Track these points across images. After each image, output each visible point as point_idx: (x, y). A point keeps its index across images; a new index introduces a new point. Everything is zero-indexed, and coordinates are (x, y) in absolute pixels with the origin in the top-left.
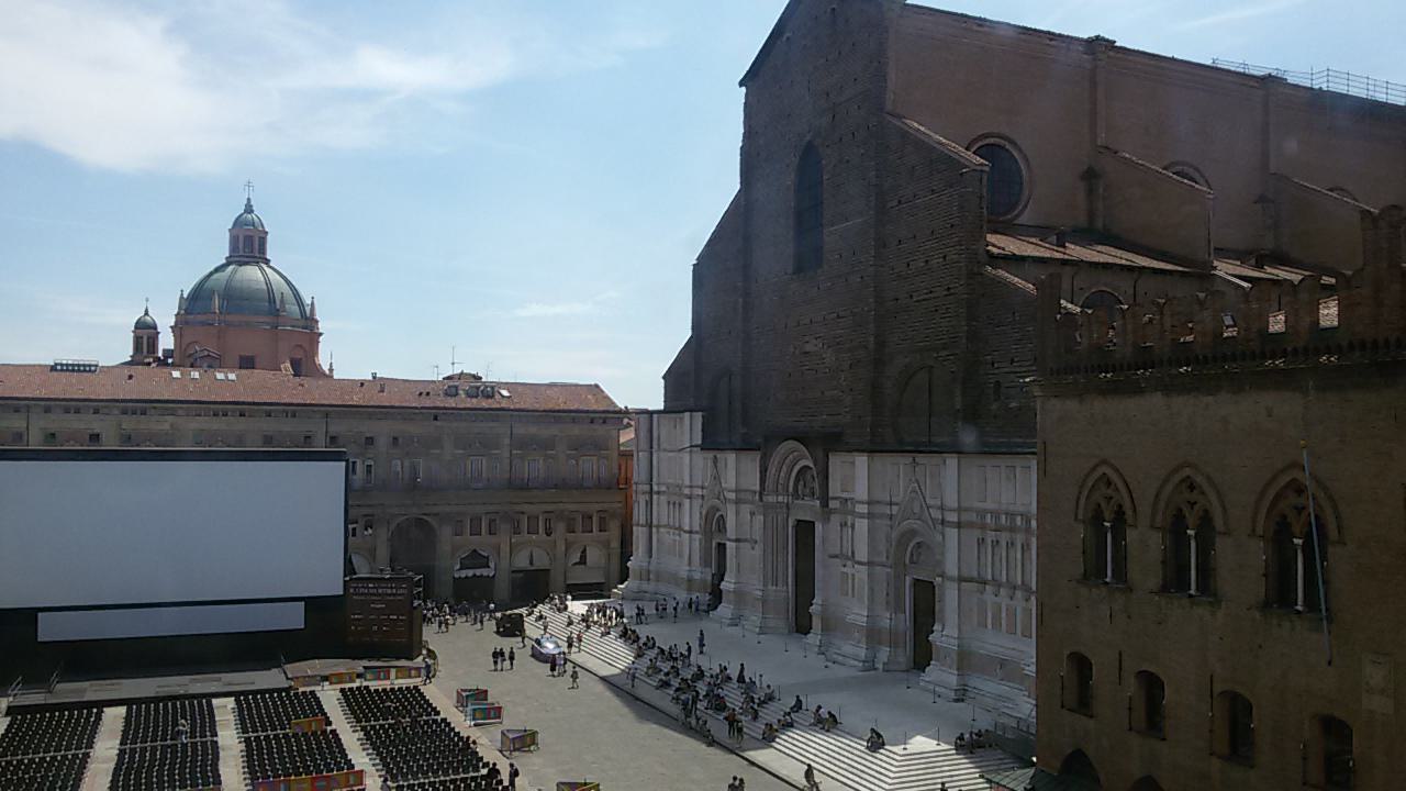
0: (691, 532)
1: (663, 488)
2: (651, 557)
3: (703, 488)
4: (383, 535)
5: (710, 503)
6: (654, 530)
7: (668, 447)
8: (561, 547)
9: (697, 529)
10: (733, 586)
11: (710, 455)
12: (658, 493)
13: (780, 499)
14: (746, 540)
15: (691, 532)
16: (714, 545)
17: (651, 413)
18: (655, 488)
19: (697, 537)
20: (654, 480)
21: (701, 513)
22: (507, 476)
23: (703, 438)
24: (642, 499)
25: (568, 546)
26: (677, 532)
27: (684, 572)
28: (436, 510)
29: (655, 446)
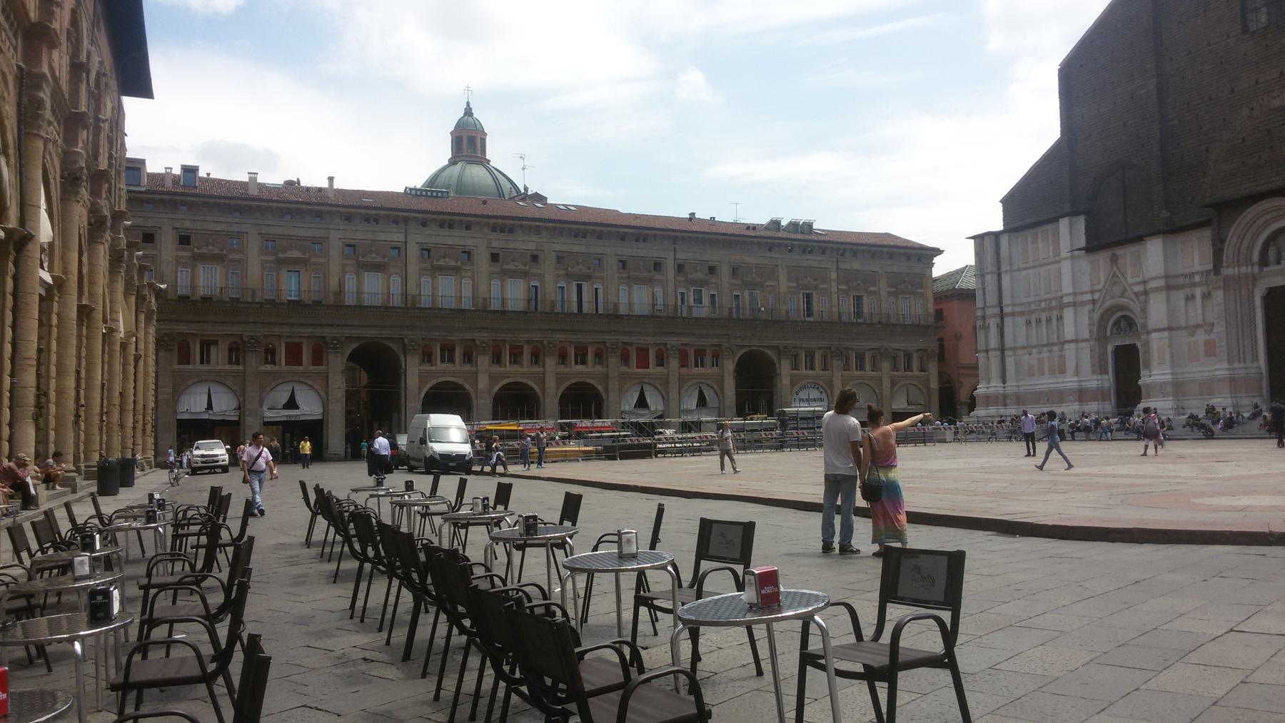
0: (1076, 341)
1: (1018, 309)
2: (1004, 382)
3: (1092, 292)
4: (730, 366)
5: (1108, 304)
6: (1008, 353)
7: (1022, 266)
8: (886, 383)
9: (1087, 336)
10: (1169, 377)
11: (1103, 257)
12: (1013, 314)
13: (1243, 270)
14: (1179, 328)
15: (1076, 341)
16: (1110, 348)
17: (996, 236)
18: (1007, 310)
19: (1084, 345)
20: (1007, 301)
21: (1090, 318)
22: (835, 310)
23: (1087, 242)
24: (993, 323)
25: (893, 384)
26: (1045, 349)
27: (1075, 385)
28: (775, 343)
29: (1004, 267)
